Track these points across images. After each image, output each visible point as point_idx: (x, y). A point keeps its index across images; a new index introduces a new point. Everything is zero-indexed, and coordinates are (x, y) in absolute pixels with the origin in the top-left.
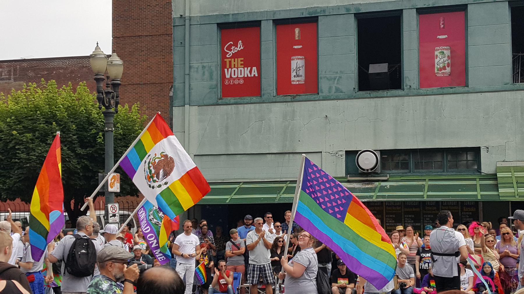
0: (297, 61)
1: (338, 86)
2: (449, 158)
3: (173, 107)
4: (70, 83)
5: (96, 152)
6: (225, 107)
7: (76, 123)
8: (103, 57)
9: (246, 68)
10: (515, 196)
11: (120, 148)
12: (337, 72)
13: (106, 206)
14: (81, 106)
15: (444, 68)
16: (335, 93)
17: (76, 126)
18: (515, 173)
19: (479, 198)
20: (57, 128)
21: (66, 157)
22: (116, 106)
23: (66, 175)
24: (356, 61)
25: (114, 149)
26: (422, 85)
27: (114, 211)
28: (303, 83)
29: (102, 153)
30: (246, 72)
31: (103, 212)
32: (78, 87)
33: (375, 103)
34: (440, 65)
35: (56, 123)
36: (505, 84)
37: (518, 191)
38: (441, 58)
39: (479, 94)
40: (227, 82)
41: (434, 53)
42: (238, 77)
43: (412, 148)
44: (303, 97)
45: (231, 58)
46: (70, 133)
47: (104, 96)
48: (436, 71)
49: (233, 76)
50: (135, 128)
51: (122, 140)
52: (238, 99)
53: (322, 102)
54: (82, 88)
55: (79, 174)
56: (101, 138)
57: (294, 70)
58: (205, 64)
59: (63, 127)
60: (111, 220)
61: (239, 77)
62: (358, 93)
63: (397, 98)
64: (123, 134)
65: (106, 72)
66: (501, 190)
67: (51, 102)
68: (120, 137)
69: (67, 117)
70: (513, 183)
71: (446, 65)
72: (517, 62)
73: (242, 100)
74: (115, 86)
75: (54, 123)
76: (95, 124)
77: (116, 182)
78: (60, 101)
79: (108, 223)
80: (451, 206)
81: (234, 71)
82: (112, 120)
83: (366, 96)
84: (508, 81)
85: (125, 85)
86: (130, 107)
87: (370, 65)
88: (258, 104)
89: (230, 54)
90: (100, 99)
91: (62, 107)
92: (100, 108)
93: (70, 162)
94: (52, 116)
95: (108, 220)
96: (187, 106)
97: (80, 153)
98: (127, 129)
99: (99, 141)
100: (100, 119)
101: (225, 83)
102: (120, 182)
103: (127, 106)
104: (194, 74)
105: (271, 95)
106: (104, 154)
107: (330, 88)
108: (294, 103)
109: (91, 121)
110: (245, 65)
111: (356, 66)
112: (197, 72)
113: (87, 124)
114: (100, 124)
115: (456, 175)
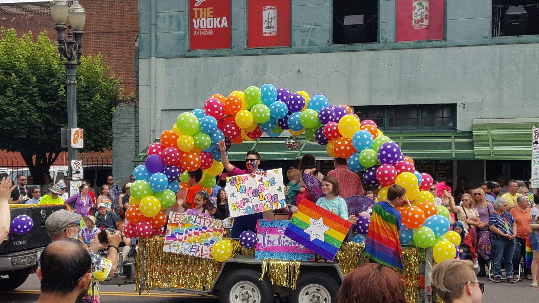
0: (269, 11)
1: (311, 38)
2: (425, 114)
3: (139, 59)
4: (30, 31)
5: (58, 105)
6: (193, 60)
7: (36, 74)
8: (65, 4)
9: (215, 19)
10: (490, 155)
11: (83, 101)
12: (311, 24)
13: (69, 162)
14: (42, 56)
15: (422, 20)
16: (308, 46)
17: (36, 78)
18: (491, 131)
19: (454, 156)
20: (16, 80)
21: (27, 111)
22: (79, 57)
23: (26, 130)
24: (330, 13)
25: (77, 103)
26: (398, 38)
27: (77, 168)
28: (275, 34)
29: (64, 106)
30: (214, 23)
31: (66, 168)
32: (39, 36)
33: (350, 57)
34: (418, 17)
35: (15, 75)
36: (484, 38)
37: (494, 149)
38: (418, 9)
39: (457, 48)
40: (195, 33)
41: (412, 5)
42: (206, 28)
43: (386, 104)
44: (275, 50)
45: (199, 7)
46: (30, 85)
47: (66, 46)
48: (413, 23)
49: (202, 27)
50: (99, 80)
51: (86, 93)
52: (206, 52)
53: (294, 55)
54: (43, 37)
55: (40, 128)
56: (63, 90)
57: (266, 21)
58: (172, 14)
59: (23, 79)
60: (74, 177)
61: (208, 28)
62: (332, 46)
63: (372, 52)
64: (86, 87)
65: (68, 20)
66: (476, 149)
67: (10, 52)
68: (82, 89)
69: (27, 68)
70: (488, 141)
71: (424, 17)
72: (497, 14)
73: (211, 53)
74: (77, 36)
75: (13, 74)
76: (57, 76)
77: (79, 138)
78: (19, 50)
79: (71, 180)
80: (425, 164)
81: (203, 21)
82: (74, 72)
83: (340, 49)
84: (487, 35)
85: (88, 33)
86: (93, 57)
87: (345, 16)
88: (227, 57)
89: (199, 3)
90: (61, 50)
91: (21, 57)
92: (62, 60)
93: (30, 115)
94: (11, 66)
95: (71, 177)
96: (153, 58)
97: (41, 106)
98: (90, 82)
99: (61, 94)
100: (62, 70)
101: (194, 34)
102: (84, 137)
103: (89, 57)
104: (160, 24)
105: (241, 48)
106: (66, 107)
107: (303, 40)
108: (266, 56)
109: (52, 73)
110: (215, 15)
111: (330, 17)
112: (164, 21)
113: (49, 76)
114: (61, 75)
115: (431, 132)
